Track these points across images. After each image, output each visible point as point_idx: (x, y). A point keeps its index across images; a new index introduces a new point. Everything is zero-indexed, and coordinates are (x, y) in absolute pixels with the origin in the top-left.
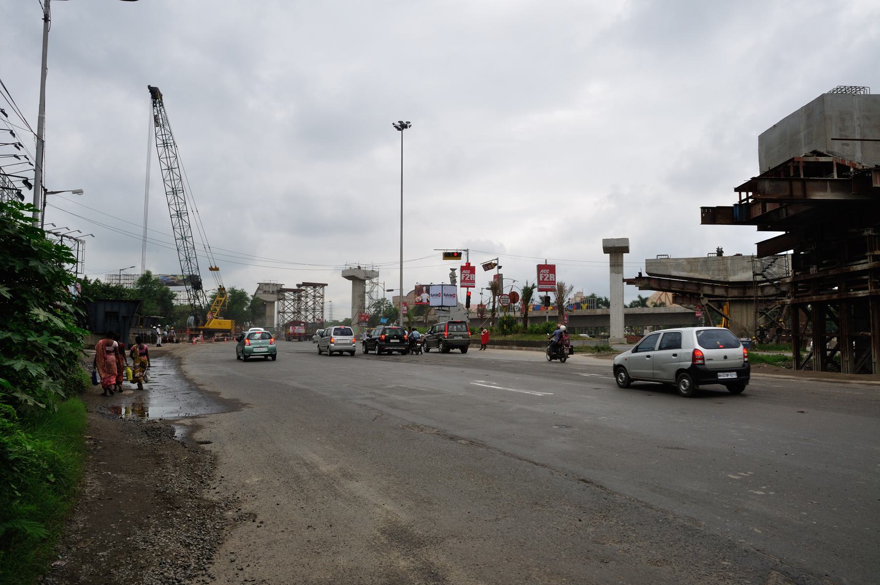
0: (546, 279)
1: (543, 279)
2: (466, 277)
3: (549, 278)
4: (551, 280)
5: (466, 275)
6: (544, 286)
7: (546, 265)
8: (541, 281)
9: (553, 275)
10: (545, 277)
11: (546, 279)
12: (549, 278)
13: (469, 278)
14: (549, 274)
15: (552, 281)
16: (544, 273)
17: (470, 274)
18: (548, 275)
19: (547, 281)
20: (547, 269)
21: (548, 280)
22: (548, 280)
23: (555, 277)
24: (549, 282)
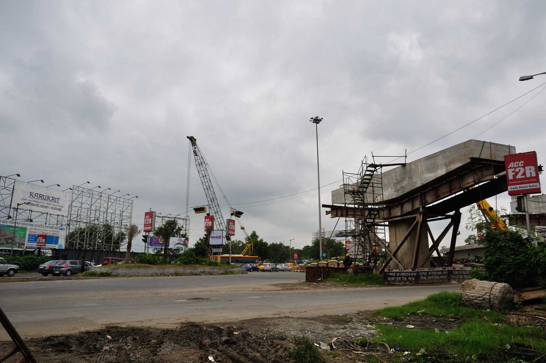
0: (519, 176)
1: (514, 176)
3: (524, 174)
4: (528, 175)
5: (517, 170)
6: (518, 186)
7: (510, 155)
8: (511, 180)
10: (517, 173)
12: (524, 174)
15: (531, 178)
17: (524, 167)
18: (522, 170)
21: (524, 177)
22: (524, 177)
24: (526, 178)
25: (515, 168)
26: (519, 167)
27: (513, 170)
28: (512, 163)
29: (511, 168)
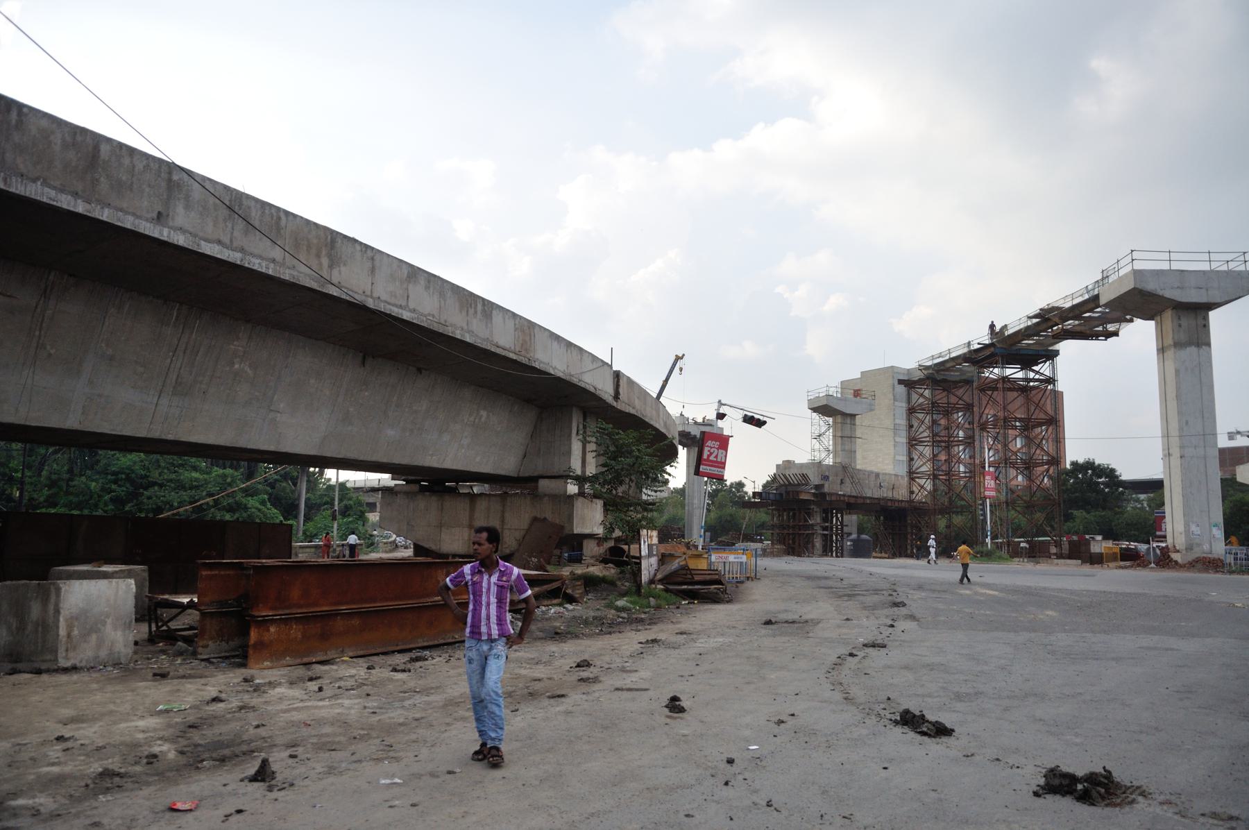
0: (712, 458)
1: (709, 456)
2: (711, 454)
4: (719, 460)
5: (712, 451)
6: (708, 468)
9: (724, 452)
11: (712, 458)
12: (716, 457)
13: (716, 457)
14: (718, 449)
16: (711, 448)
19: (712, 461)
20: (716, 441)
21: (715, 459)
23: (726, 456)
24: (716, 462)
25: (711, 448)
26: (714, 447)
27: (709, 449)
28: (710, 442)
29: (708, 446)
